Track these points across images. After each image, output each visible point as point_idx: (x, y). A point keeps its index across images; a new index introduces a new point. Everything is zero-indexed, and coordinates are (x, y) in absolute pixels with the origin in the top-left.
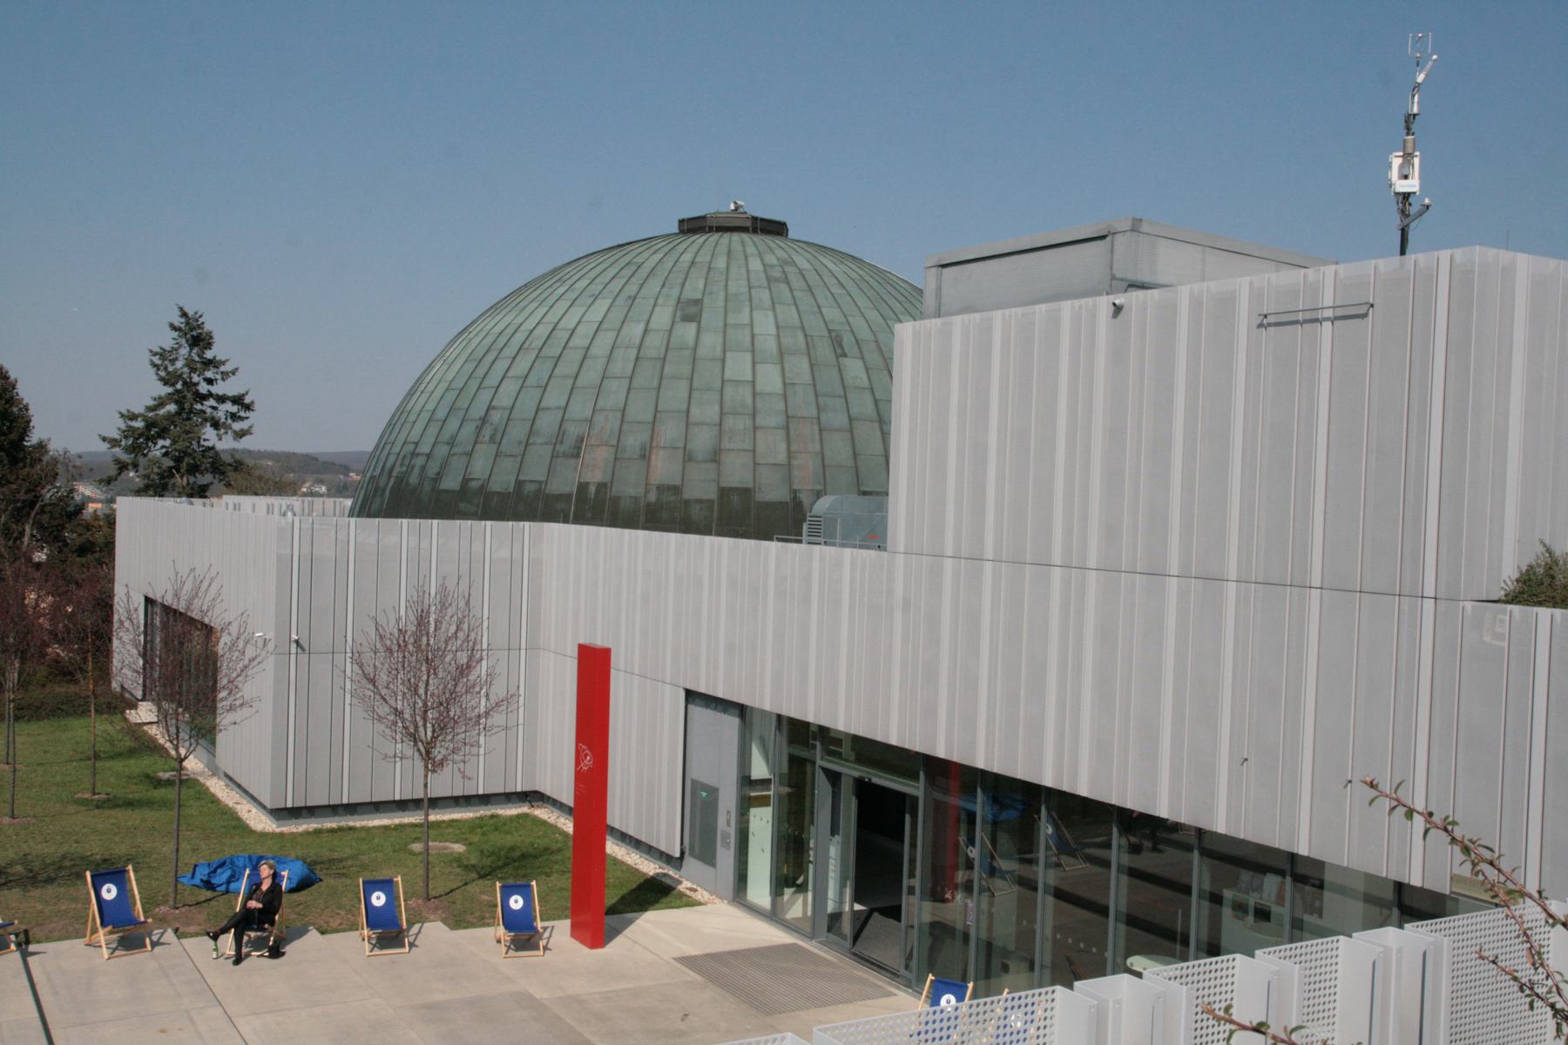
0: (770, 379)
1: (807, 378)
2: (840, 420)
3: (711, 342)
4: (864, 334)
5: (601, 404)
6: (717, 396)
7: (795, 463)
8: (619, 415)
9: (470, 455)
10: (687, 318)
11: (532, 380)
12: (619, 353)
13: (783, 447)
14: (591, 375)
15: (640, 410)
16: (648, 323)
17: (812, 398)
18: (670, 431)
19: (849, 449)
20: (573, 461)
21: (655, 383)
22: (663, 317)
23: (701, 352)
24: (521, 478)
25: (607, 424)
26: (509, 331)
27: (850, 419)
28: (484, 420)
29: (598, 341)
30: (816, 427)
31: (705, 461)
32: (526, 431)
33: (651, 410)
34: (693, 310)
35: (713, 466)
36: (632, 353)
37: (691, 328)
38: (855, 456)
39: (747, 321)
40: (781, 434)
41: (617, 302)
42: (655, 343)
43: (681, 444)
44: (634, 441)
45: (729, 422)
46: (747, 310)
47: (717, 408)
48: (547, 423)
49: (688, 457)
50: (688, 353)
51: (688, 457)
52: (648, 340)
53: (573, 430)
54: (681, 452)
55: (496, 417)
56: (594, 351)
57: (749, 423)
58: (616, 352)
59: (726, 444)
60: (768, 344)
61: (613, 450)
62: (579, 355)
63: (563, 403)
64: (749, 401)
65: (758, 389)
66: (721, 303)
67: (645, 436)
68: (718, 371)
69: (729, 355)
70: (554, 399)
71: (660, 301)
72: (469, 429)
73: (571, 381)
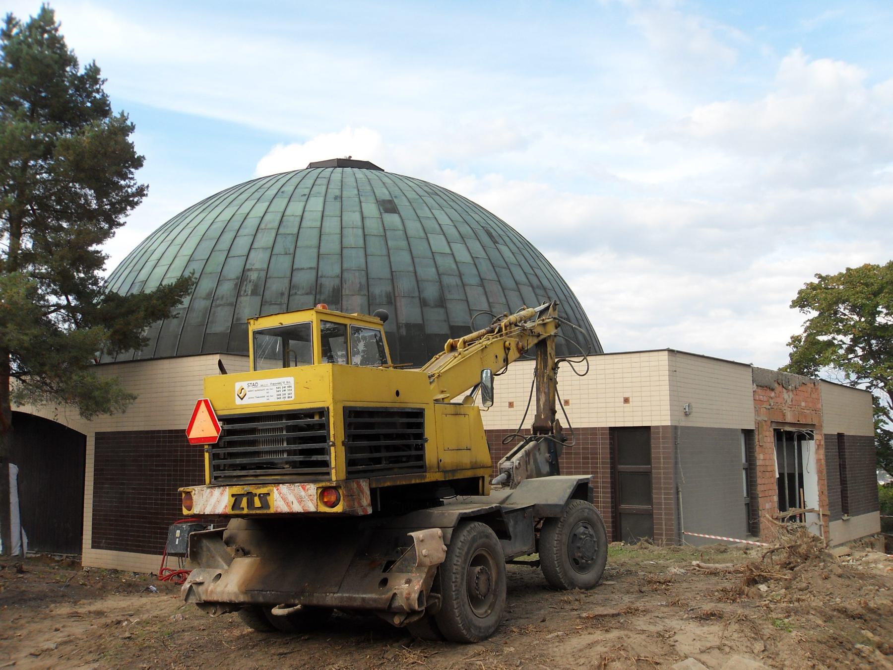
0: (462, 255)
1: (483, 254)
3: (413, 227)
5: (345, 266)
6: (431, 261)
9: (234, 305)
10: (387, 211)
13: (484, 299)
14: (331, 245)
15: (378, 268)
16: (362, 212)
18: (405, 284)
21: (384, 252)
22: (371, 209)
23: (410, 233)
25: (353, 280)
26: (238, 218)
27: (517, 284)
28: (242, 278)
29: (326, 224)
31: (436, 306)
32: (287, 285)
33: (388, 270)
34: (389, 206)
35: (442, 311)
36: (360, 232)
42: (373, 225)
43: (417, 294)
45: (446, 280)
46: (426, 208)
47: (434, 270)
49: (424, 303)
51: (424, 303)
52: (368, 223)
53: (329, 284)
54: (418, 299)
55: (253, 276)
58: (345, 231)
59: (448, 296)
61: (365, 298)
62: (316, 233)
63: (314, 265)
64: (454, 266)
65: (458, 259)
66: (408, 204)
67: (389, 288)
69: (429, 235)
70: (305, 260)
71: (362, 199)
72: (226, 288)
73: (316, 250)
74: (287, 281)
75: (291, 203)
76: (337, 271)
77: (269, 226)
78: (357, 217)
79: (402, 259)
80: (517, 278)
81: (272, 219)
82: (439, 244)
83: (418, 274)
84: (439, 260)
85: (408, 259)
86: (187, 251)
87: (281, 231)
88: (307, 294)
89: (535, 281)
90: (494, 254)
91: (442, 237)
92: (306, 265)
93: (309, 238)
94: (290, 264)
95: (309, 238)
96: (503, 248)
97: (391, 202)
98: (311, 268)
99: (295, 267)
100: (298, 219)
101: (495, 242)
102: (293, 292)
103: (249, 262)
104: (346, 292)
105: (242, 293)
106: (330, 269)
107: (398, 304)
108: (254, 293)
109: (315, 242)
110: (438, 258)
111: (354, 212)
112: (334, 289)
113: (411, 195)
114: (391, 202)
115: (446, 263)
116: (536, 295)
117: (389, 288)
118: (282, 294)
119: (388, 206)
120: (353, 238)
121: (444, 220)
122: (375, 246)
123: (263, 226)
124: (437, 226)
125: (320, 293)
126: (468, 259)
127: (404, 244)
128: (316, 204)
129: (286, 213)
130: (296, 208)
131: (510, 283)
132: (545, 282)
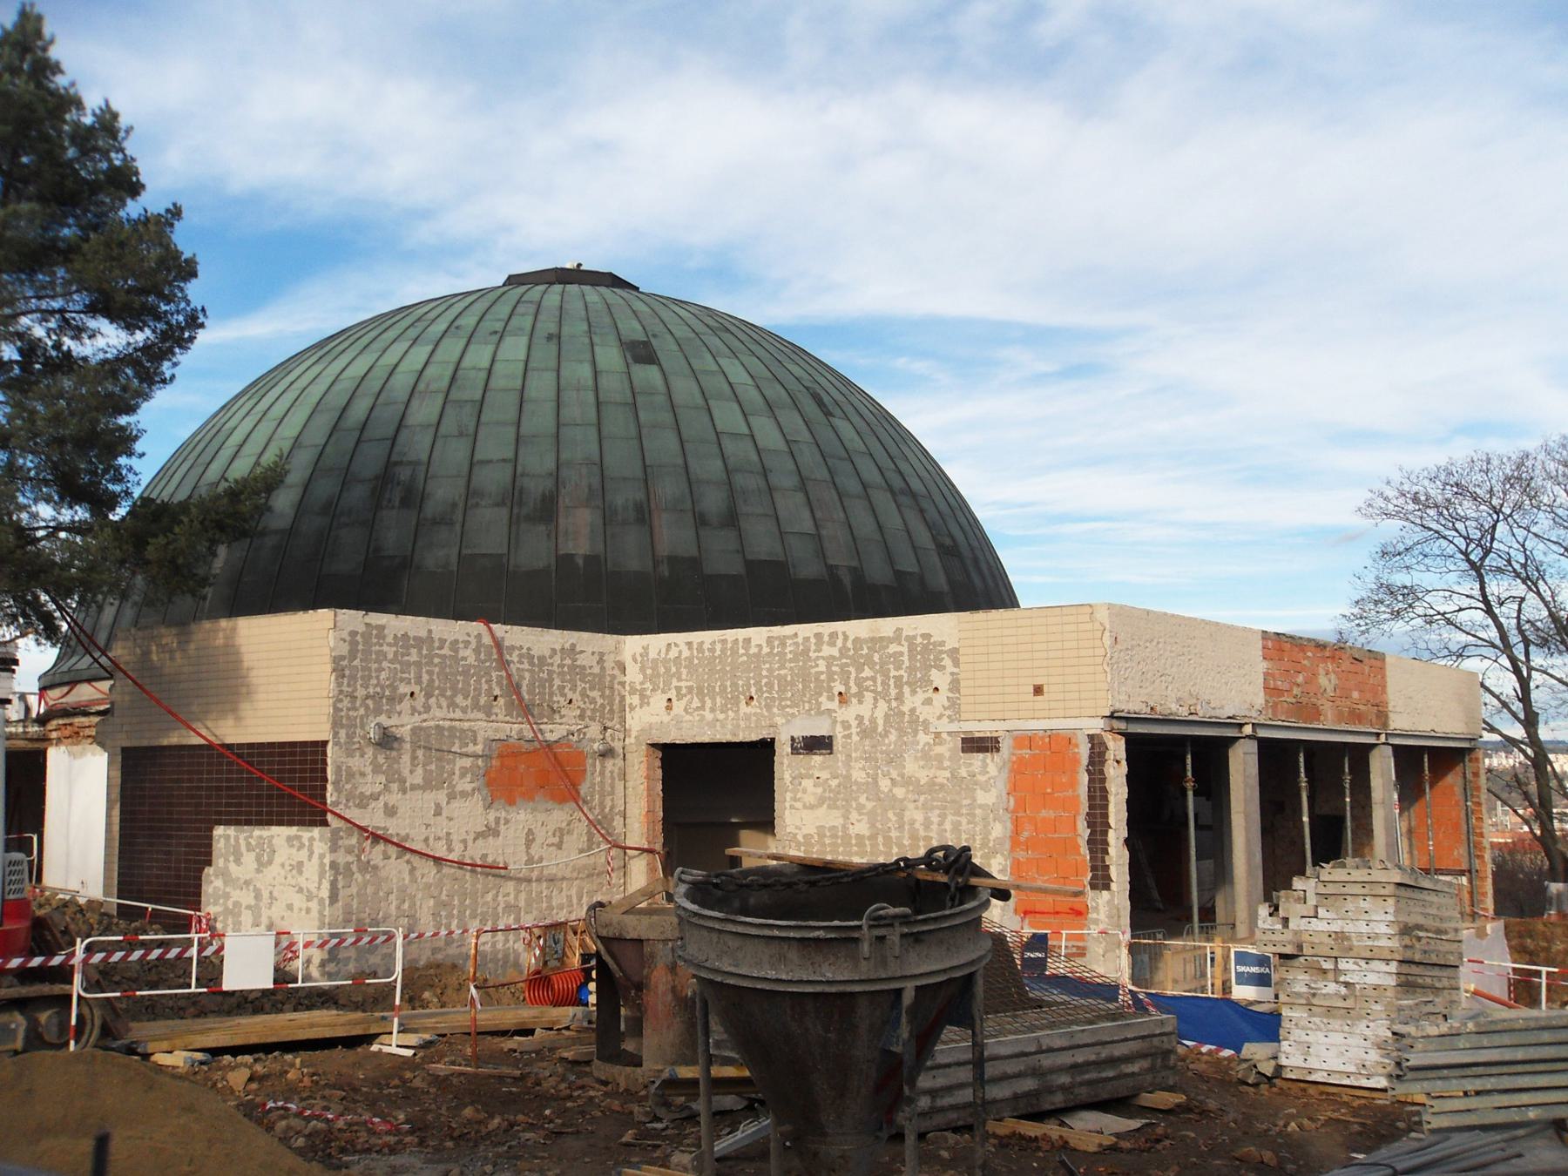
0: (768, 435)
1: (806, 436)
2: (852, 486)
3: (684, 389)
4: (839, 397)
5: (564, 456)
7: (824, 532)
8: (596, 469)
11: (448, 426)
12: (569, 396)
13: (806, 514)
14: (540, 420)
15: (621, 460)
16: (594, 363)
17: (818, 457)
18: (668, 488)
19: (872, 519)
20: (542, 528)
21: (633, 432)
22: (610, 357)
23: (677, 399)
24: (464, 552)
30: (833, 491)
32: (463, 491)
33: (640, 463)
37: (652, 372)
38: (880, 528)
39: (715, 368)
40: (800, 497)
41: (535, 340)
42: (613, 385)
43: (689, 505)
44: (624, 497)
45: (740, 480)
46: (709, 356)
47: (719, 463)
48: (493, 479)
49: (701, 521)
50: (661, 399)
51: (701, 521)
52: (604, 382)
53: (536, 487)
54: (690, 514)
56: (532, 392)
57: (762, 483)
58: (565, 396)
59: (743, 509)
60: (751, 395)
62: (513, 399)
63: (510, 454)
64: (755, 457)
66: (675, 347)
68: (707, 419)
69: (711, 402)
70: (495, 446)
71: (596, 339)
73: (512, 430)
74: (462, 482)
75: (472, 347)
76: (549, 464)
77: (434, 386)
78: (585, 371)
79: (663, 446)
80: (866, 476)
81: (439, 374)
82: (728, 417)
83: (691, 470)
84: (728, 445)
85: (674, 444)
86: (290, 430)
87: (454, 395)
88: (497, 505)
89: (897, 483)
90: (825, 434)
91: (735, 406)
92: (495, 455)
93: (501, 409)
94: (468, 453)
95: (501, 409)
96: (840, 424)
97: (647, 344)
98: (504, 460)
99: (478, 457)
100: (484, 375)
101: (828, 414)
102: (471, 502)
103: (396, 449)
104: (565, 500)
105: (385, 503)
106: (538, 461)
107: (656, 523)
108: (406, 502)
109: (512, 414)
110: (726, 442)
111: (581, 362)
112: (544, 495)
113: (681, 332)
114: (647, 344)
115: (739, 451)
116: (898, 507)
117: (640, 496)
118: (454, 505)
119: (642, 353)
120: (579, 408)
121: (738, 375)
122: (618, 423)
123: (421, 386)
124: (726, 387)
125: (521, 503)
126: (782, 446)
127: (667, 417)
128: (514, 348)
129: (463, 365)
130: (480, 356)
131: (852, 486)
132: (916, 485)
